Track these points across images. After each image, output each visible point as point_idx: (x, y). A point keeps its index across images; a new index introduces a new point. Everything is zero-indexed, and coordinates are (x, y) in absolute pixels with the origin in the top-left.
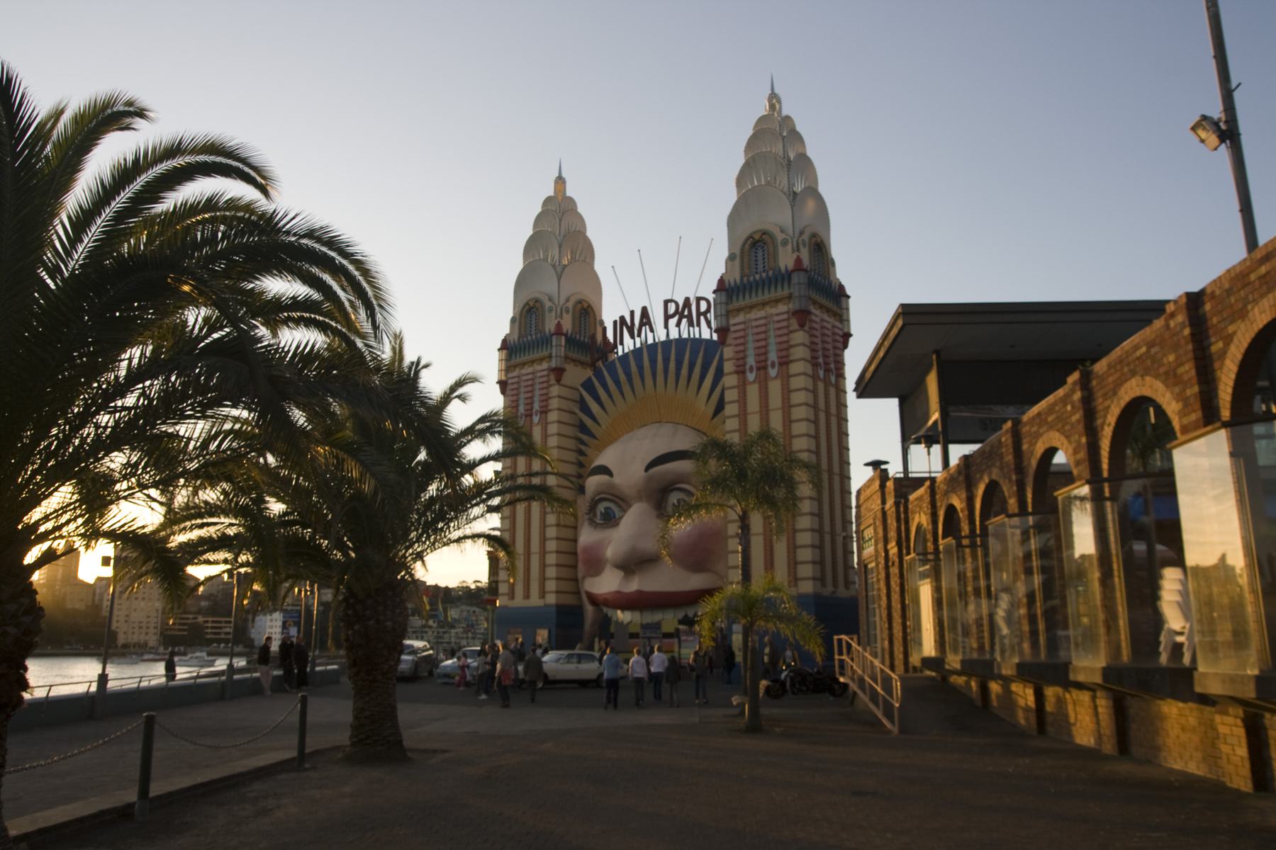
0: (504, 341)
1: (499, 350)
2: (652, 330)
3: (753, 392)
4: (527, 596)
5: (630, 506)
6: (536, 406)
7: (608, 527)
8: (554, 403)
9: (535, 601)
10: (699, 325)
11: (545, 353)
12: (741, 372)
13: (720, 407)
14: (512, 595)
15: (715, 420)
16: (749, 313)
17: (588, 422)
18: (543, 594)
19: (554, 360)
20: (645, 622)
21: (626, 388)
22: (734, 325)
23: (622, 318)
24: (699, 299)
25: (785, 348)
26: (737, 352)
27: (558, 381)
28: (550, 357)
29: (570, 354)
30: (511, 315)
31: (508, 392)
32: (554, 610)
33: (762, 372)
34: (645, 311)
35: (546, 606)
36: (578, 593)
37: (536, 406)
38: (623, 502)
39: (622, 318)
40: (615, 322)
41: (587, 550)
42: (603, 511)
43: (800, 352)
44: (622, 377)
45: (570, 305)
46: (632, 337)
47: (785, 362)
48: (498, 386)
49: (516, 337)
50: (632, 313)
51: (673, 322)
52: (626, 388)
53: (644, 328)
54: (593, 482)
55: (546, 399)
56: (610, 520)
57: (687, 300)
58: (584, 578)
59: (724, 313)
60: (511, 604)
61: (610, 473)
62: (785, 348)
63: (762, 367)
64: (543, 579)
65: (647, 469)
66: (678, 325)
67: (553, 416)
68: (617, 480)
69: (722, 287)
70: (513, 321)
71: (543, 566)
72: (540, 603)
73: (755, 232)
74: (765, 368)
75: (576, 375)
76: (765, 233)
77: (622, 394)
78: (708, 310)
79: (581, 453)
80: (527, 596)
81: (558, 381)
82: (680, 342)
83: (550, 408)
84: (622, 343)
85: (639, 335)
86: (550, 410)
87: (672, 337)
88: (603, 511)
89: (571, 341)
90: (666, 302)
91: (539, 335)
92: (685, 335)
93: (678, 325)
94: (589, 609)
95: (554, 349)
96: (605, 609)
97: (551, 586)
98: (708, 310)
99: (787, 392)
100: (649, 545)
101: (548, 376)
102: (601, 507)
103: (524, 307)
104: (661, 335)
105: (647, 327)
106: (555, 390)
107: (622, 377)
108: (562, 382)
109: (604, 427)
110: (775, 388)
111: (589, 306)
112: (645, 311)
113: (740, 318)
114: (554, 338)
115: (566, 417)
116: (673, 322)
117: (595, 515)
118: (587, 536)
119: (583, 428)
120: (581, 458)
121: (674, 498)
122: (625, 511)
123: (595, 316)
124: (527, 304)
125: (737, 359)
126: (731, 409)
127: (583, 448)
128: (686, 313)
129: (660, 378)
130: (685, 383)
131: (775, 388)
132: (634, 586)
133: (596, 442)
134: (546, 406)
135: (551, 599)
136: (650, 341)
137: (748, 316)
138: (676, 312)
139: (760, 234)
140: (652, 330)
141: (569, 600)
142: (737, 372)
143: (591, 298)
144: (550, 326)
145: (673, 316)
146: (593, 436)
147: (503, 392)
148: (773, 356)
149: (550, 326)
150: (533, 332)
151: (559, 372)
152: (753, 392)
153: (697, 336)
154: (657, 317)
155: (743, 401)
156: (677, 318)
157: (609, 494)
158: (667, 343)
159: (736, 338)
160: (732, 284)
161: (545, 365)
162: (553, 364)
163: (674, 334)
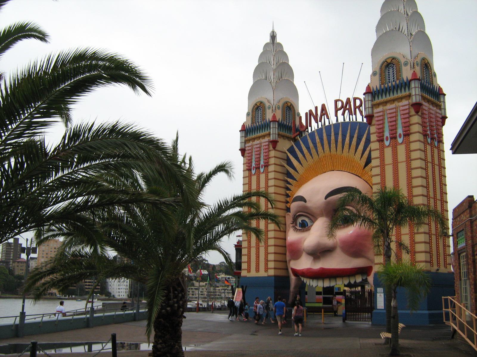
0: (243, 126)
1: (240, 131)
2: (328, 118)
3: (388, 152)
4: (257, 270)
5: (316, 219)
6: (262, 163)
7: (304, 231)
8: (272, 161)
9: (262, 273)
10: (355, 114)
11: (267, 132)
12: (381, 140)
13: (369, 161)
14: (249, 270)
16: (386, 105)
17: (291, 170)
18: (266, 269)
19: (271, 136)
20: (325, 286)
21: (313, 151)
22: (377, 113)
23: (311, 111)
24: (355, 99)
25: (407, 127)
26: (378, 129)
27: (274, 148)
28: (269, 134)
29: (281, 133)
30: (246, 111)
31: (246, 155)
32: (273, 278)
33: (393, 140)
34: (324, 108)
36: (287, 269)
37: (262, 163)
38: (313, 217)
39: (311, 111)
40: (306, 114)
41: (292, 244)
43: (416, 128)
44: (311, 145)
45: (281, 105)
46: (317, 122)
47: (407, 134)
48: (240, 152)
49: (249, 123)
51: (340, 113)
52: (313, 151)
53: (323, 116)
54: (294, 206)
55: (267, 158)
56: (304, 227)
57: (348, 100)
58: (290, 261)
59: (370, 106)
60: (248, 275)
61: (305, 201)
62: (407, 127)
63: (393, 137)
64: (267, 261)
65: (326, 198)
67: (271, 168)
68: (308, 204)
69: (369, 92)
70: (248, 114)
72: (265, 275)
73: (388, 58)
74: (395, 138)
75: (284, 145)
76: (394, 58)
77: (311, 155)
78: (361, 105)
79: (288, 189)
80: (257, 270)
82: (345, 124)
84: (311, 126)
85: (321, 121)
86: (269, 165)
87: (339, 121)
89: (281, 126)
90: (336, 101)
91: (263, 122)
92: (347, 120)
93: (343, 114)
94: (293, 278)
95: (272, 129)
96: (302, 279)
97: (271, 265)
98: (361, 105)
99: (408, 151)
100: (328, 242)
101: (268, 145)
102: (300, 220)
103: (254, 107)
104: (333, 120)
105: (325, 116)
106: (272, 153)
107: (311, 145)
108: (276, 149)
110: (401, 150)
111: (291, 105)
112: (324, 108)
113: (381, 109)
114: (272, 123)
115: (279, 169)
116: (340, 113)
117: (296, 225)
118: (292, 236)
119: (289, 175)
120: (288, 192)
122: (313, 222)
123: (294, 110)
124: (256, 104)
125: (379, 133)
126: (375, 162)
128: (348, 107)
129: (333, 145)
131: (401, 150)
132: (318, 266)
134: (268, 163)
135: (271, 272)
136: (327, 124)
137: (385, 108)
138: (342, 107)
139: (391, 59)
140: (328, 118)
141: (281, 273)
142: (378, 141)
143: (292, 100)
144: (269, 116)
145: (340, 109)
146: (295, 180)
147: (243, 155)
148: (400, 131)
149: (269, 116)
150: (260, 121)
151: (274, 143)
152: (388, 152)
153: (354, 120)
154: (331, 110)
155: (382, 158)
157: (304, 212)
158: (337, 125)
159: (378, 121)
160: (375, 89)
161: (266, 139)
162: (271, 138)
163: (341, 119)
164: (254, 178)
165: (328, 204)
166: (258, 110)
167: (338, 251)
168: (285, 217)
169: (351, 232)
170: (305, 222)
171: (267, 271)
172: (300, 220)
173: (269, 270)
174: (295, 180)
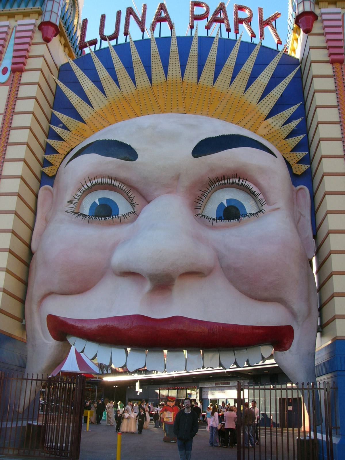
2: (171, 28)
11: (37, 7)
15: (270, 120)
17: (74, 99)
23: (130, 11)
26: (328, 40)
34: (162, 7)
40: (119, 13)
46: (143, 31)
50: (145, 6)
57: (222, 8)
66: (208, 28)
79: (52, 135)
81: (47, 40)
83: (27, 67)
85: (153, 28)
93: (208, 28)
101: (33, 31)
109: (96, 108)
112: (162, 7)
120: (52, 142)
127: (58, 130)
128: (219, 16)
130: (230, 75)
133: (80, 124)
142: (332, 62)
146: (77, 116)
156: (205, 22)
168: (36, 196)
172: (95, 198)
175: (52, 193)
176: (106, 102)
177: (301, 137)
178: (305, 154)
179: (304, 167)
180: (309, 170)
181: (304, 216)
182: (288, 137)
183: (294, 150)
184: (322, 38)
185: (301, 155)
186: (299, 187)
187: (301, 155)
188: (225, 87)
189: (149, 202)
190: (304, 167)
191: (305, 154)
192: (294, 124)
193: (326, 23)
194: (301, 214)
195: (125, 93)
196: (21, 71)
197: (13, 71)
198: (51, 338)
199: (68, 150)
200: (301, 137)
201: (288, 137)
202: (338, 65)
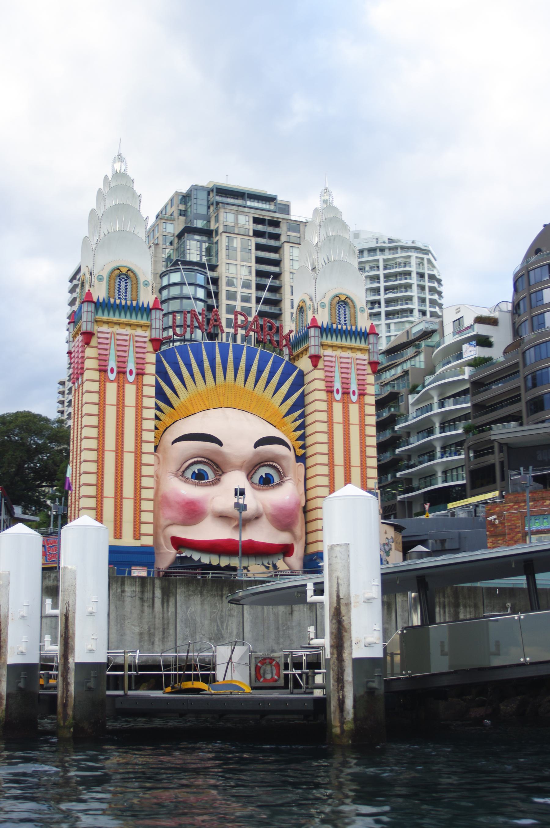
7: (264, 487)
11: (148, 323)
18: (137, 535)
35: (143, 547)
42: (197, 472)
61: (221, 444)
65: (257, 445)
68: (224, 449)
71: (138, 511)
72: (137, 543)
88: (197, 472)
97: (147, 529)
109: (182, 399)
121: (263, 471)
130: (264, 384)
133: (172, 410)
152: (338, 408)
164: (111, 389)
165: (257, 454)
166: (120, 279)
167: (264, 520)
169: (288, 497)
170: (202, 472)
171: (140, 537)
172: (196, 468)
173: (142, 537)
174: (171, 405)
175: (158, 458)
176: (188, 396)
177: (302, 432)
178: (303, 442)
179: (302, 451)
180: (305, 454)
181: (300, 481)
182: (294, 431)
183: (297, 440)
184: (322, 372)
185: (301, 443)
186: (299, 463)
187: (301, 443)
188: (261, 393)
189: (223, 473)
190: (302, 451)
191: (303, 442)
192: (299, 422)
193: (327, 363)
194: (299, 480)
195: (199, 390)
196: (143, 374)
197: (138, 374)
198: (174, 549)
199: (165, 428)
200: (302, 432)
201: (294, 431)
202: (329, 394)
